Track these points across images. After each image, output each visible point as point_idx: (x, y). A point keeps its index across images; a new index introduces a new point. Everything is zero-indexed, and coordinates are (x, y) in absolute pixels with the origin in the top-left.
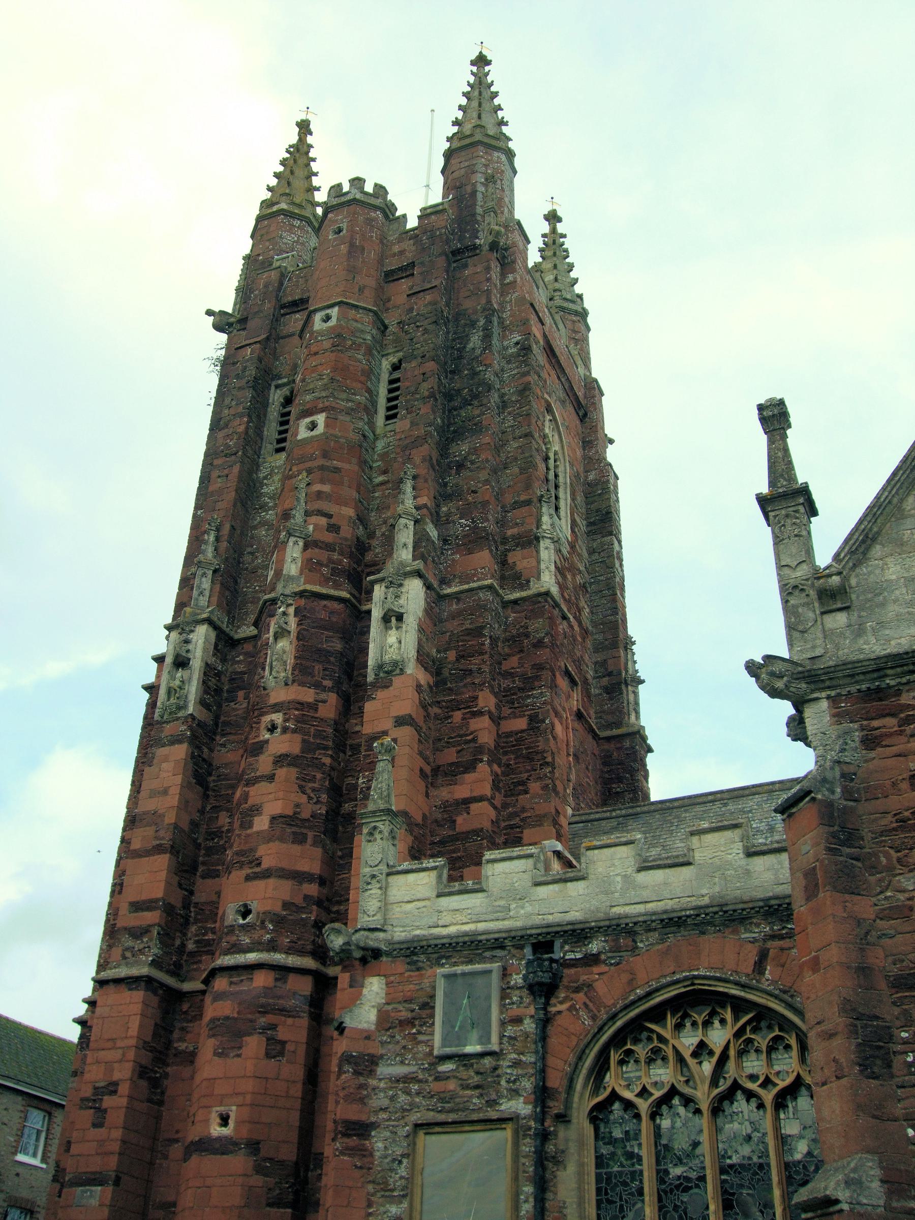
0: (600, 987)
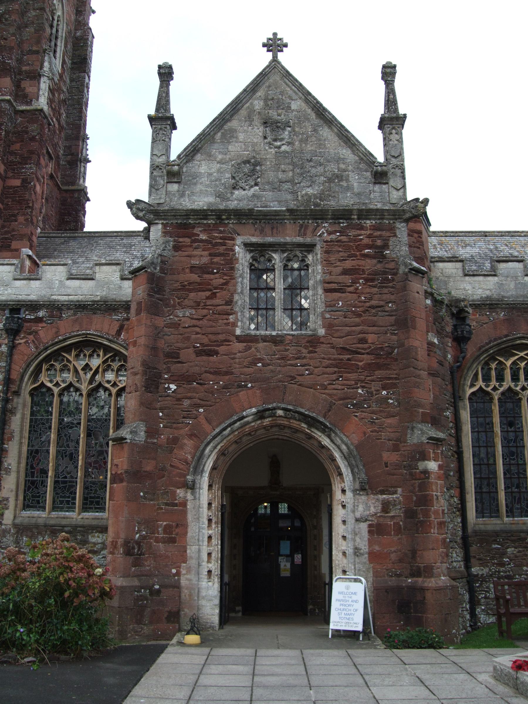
0: (42, 333)
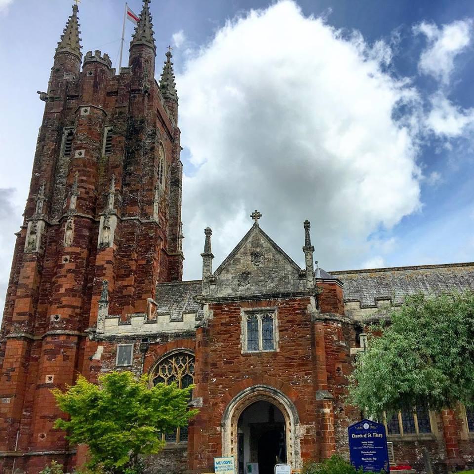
0: (158, 351)
